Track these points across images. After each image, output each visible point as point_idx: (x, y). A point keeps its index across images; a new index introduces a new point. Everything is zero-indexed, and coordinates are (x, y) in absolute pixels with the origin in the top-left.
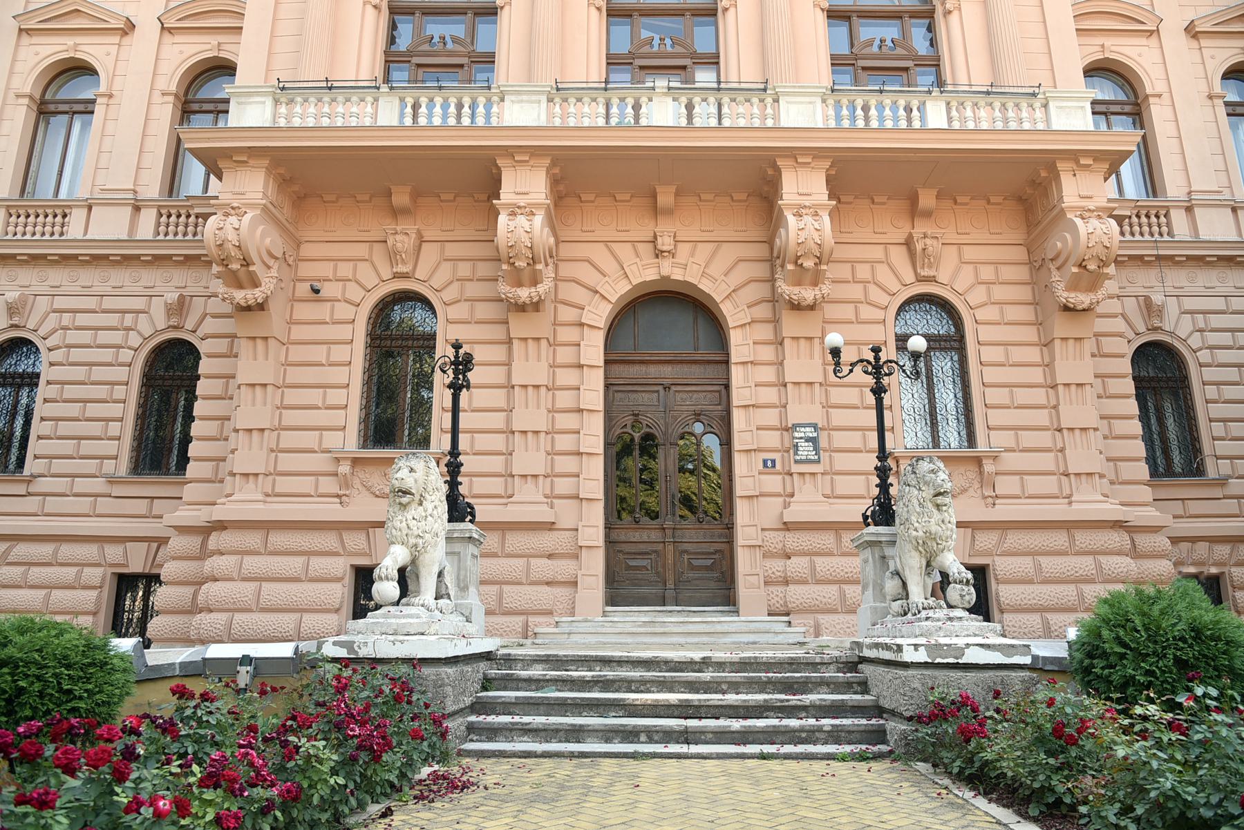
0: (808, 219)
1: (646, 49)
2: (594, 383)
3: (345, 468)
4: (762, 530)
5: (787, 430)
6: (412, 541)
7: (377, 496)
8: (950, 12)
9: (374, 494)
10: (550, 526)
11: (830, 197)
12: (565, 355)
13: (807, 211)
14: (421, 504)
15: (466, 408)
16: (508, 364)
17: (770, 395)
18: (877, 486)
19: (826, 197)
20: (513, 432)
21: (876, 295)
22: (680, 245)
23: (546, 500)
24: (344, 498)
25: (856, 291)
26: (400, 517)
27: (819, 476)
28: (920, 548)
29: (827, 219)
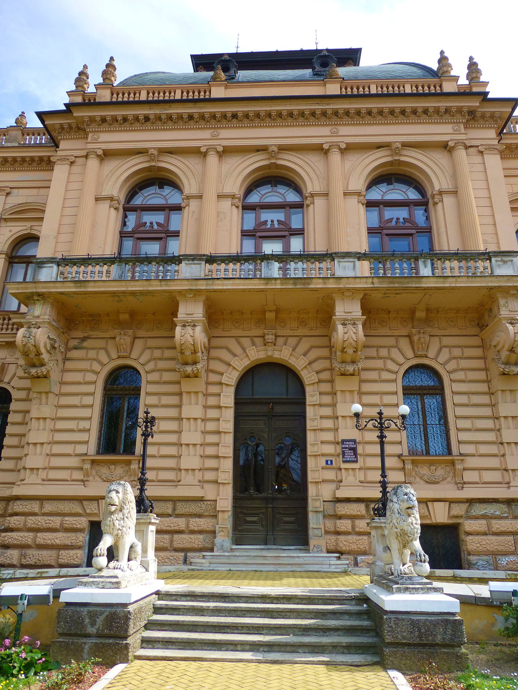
0: (350, 327)
2: (229, 414)
3: (87, 466)
6: (115, 532)
7: (104, 481)
9: (103, 479)
11: (363, 315)
12: (212, 401)
13: (349, 322)
14: (121, 511)
15: (156, 430)
18: (381, 492)
19: (361, 314)
21: (391, 365)
22: (278, 339)
24: (86, 483)
26: (109, 519)
28: (399, 538)
29: (360, 327)
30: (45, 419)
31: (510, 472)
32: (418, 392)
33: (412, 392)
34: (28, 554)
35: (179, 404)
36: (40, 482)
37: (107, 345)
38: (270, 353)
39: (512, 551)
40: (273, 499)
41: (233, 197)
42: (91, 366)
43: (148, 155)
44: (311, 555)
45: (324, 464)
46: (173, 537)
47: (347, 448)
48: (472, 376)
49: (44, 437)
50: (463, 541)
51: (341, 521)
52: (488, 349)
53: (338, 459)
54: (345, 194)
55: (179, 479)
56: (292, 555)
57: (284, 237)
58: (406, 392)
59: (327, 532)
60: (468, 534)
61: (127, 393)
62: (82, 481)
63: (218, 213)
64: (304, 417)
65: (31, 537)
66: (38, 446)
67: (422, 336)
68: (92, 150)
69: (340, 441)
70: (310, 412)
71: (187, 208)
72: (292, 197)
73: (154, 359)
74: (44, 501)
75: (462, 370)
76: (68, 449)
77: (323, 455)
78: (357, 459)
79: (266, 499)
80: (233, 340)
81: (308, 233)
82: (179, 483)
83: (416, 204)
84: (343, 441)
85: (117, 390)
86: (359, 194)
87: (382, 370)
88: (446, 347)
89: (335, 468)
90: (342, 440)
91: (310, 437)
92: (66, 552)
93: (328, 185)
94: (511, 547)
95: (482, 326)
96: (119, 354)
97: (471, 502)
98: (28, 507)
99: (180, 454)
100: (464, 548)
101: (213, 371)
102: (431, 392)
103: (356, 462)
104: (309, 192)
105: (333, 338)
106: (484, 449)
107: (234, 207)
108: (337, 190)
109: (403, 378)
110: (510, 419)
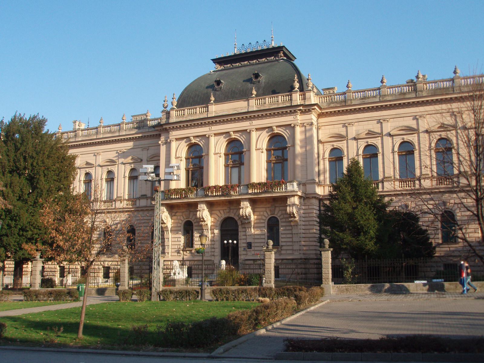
38: (228, 216)
75: (285, 218)
80: (218, 211)
84: (248, 243)
88: (281, 210)
106: (288, 244)
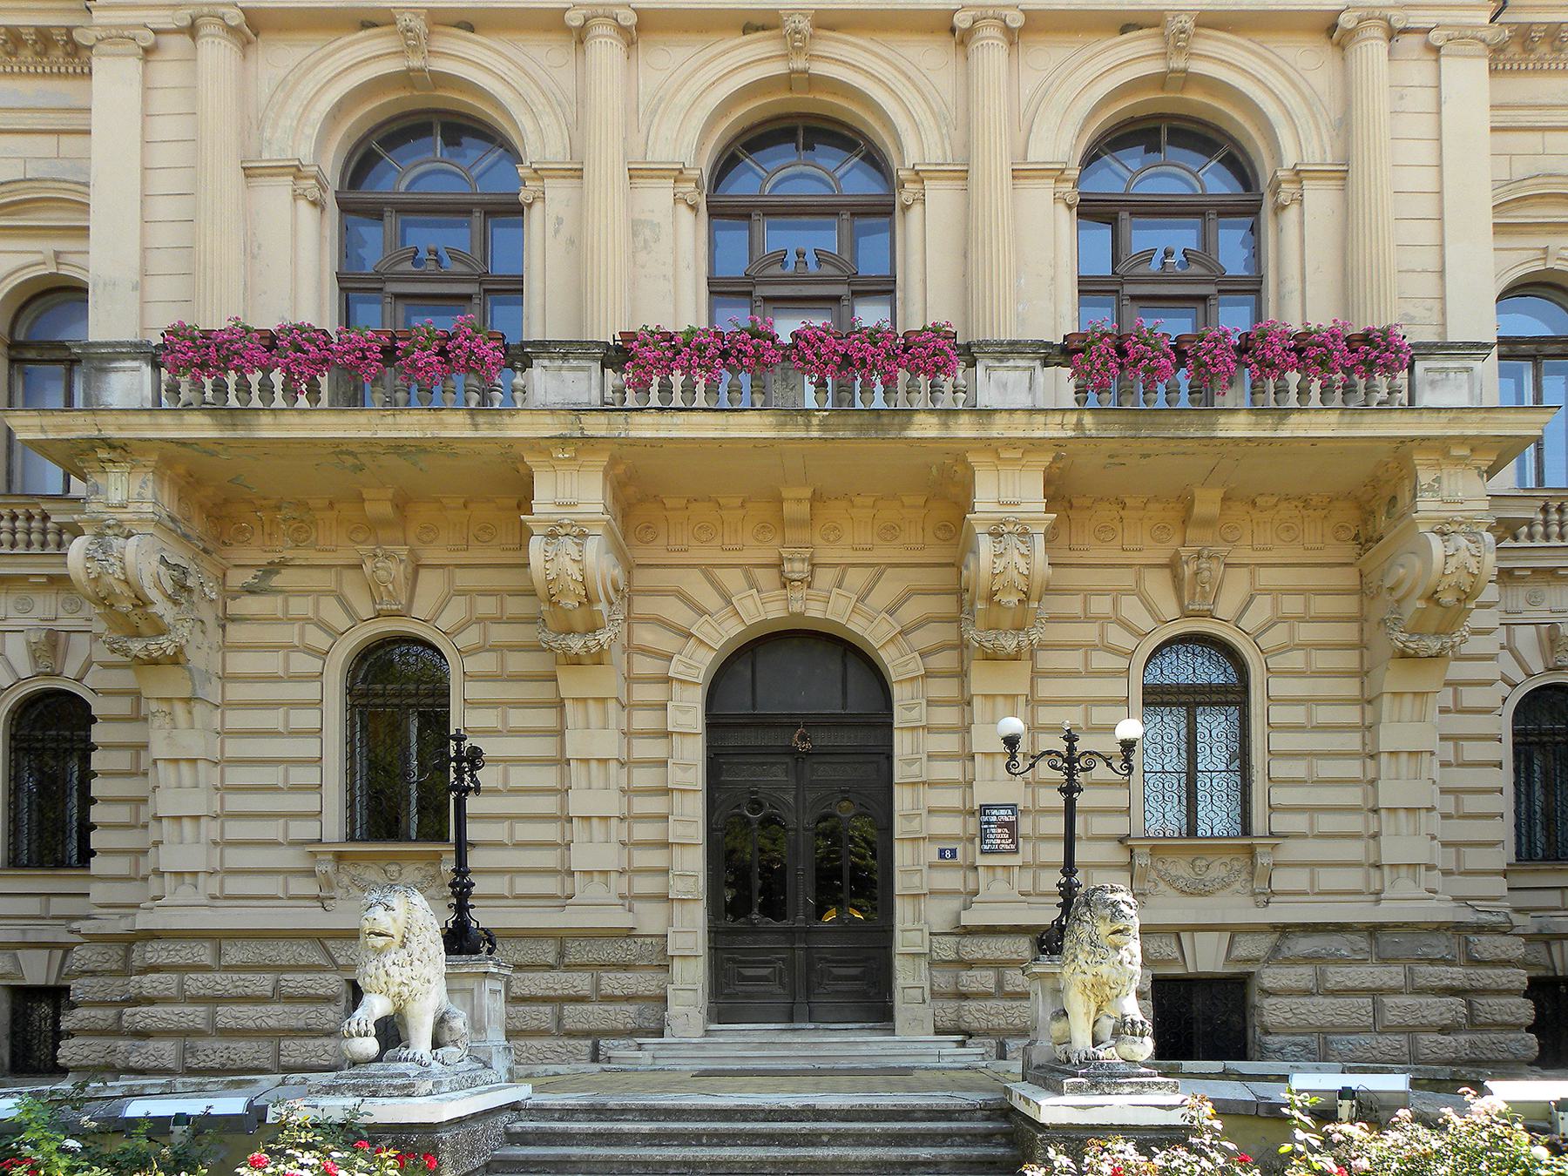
1: (776, 270)
2: (693, 751)
3: (326, 867)
4: (931, 934)
5: (973, 813)
8: (1284, 207)
10: (629, 934)
16: (560, 733)
17: (952, 770)
20: (570, 820)
21: (1117, 636)
23: (621, 902)
24: (327, 902)
25: (1089, 632)
27: (1016, 870)
30: (194, 761)
31: (1386, 870)
32: (1183, 698)
33: (1166, 698)
34: (200, 1049)
35: (558, 728)
36: (205, 902)
37: (339, 582)
39: (1365, 1026)
40: (808, 931)
41: (679, 175)
42: (302, 635)
43: (395, 33)
44: (897, 1038)
45: (935, 858)
46: (561, 1010)
47: (993, 823)
48: (1323, 660)
49: (197, 803)
50: (1255, 1007)
51: (970, 973)
52: (1372, 598)
53: (969, 847)
54: (1017, 174)
55: (568, 892)
56: (852, 1039)
57: (837, 299)
58: (1150, 699)
59: (935, 995)
60: (1268, 993)
61: (410, 701)
62: (317, 898)
63: (635, 227)
64: (889, 757)
65: (203, 1015)
66: (187, 824)
67: (1204, 566)
68: (206, 10)
69: (976, 807)
70: (902, 744)
71: (538, 206)
72: (856, 182)
73: (479, 621)
74: (224, 942)
76: (272, 830)
77: (932, 838)
78: (1017, 847)
79: (790, 933)
81: (904, 290)
82: (569, 901)
83: (1227, 210)
84: (985, 809)
85: (383, 695)
86: (1059, 175)
87: (1095, 647)
89: (962, 866)
90: (981, 806)
91: (902, 800)
92: (297, 1042)
93: (967, 146)
94: (1365, 1018)
95: (1365, 541)
96: (378, 607)
97: (1284, 930)
98: (183, 954)
99: (568, 838)
100: (1256, 1021)
101: (645, 651)
102: (1215, 698)
103: (1016, 851)
104: (909, 164)
105: (967, 567)
107: (682, 208)
108: (993, 163)
109: (1146, 666)
110: (1404, 757)
